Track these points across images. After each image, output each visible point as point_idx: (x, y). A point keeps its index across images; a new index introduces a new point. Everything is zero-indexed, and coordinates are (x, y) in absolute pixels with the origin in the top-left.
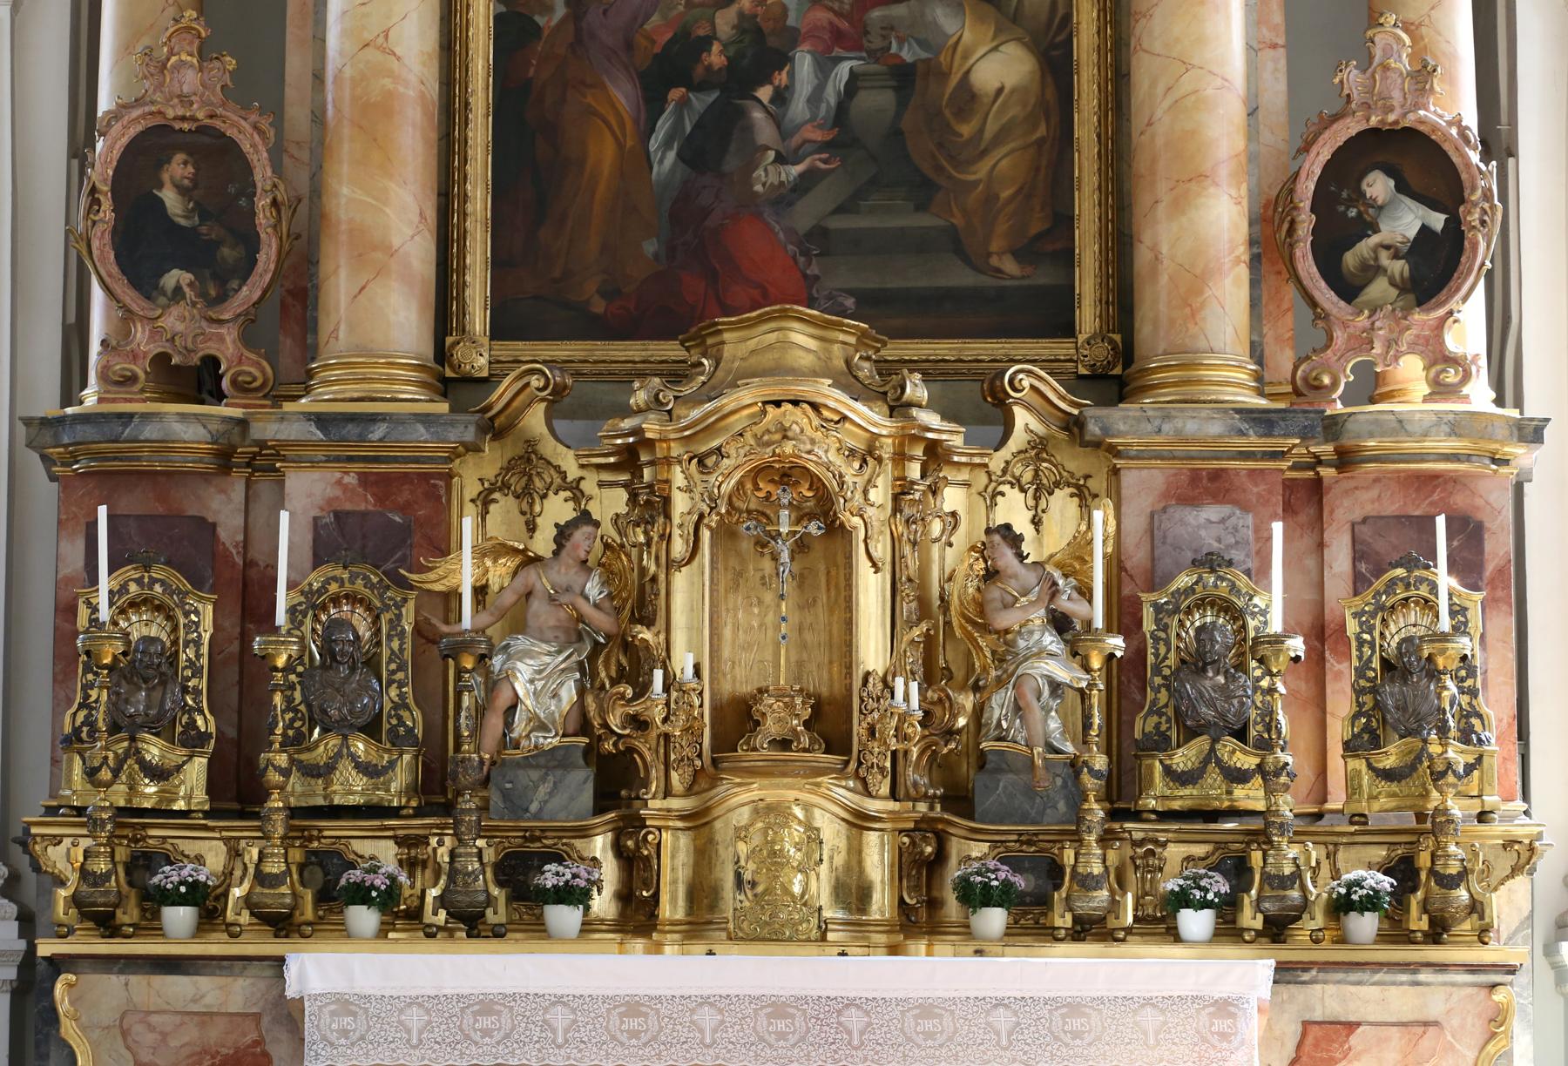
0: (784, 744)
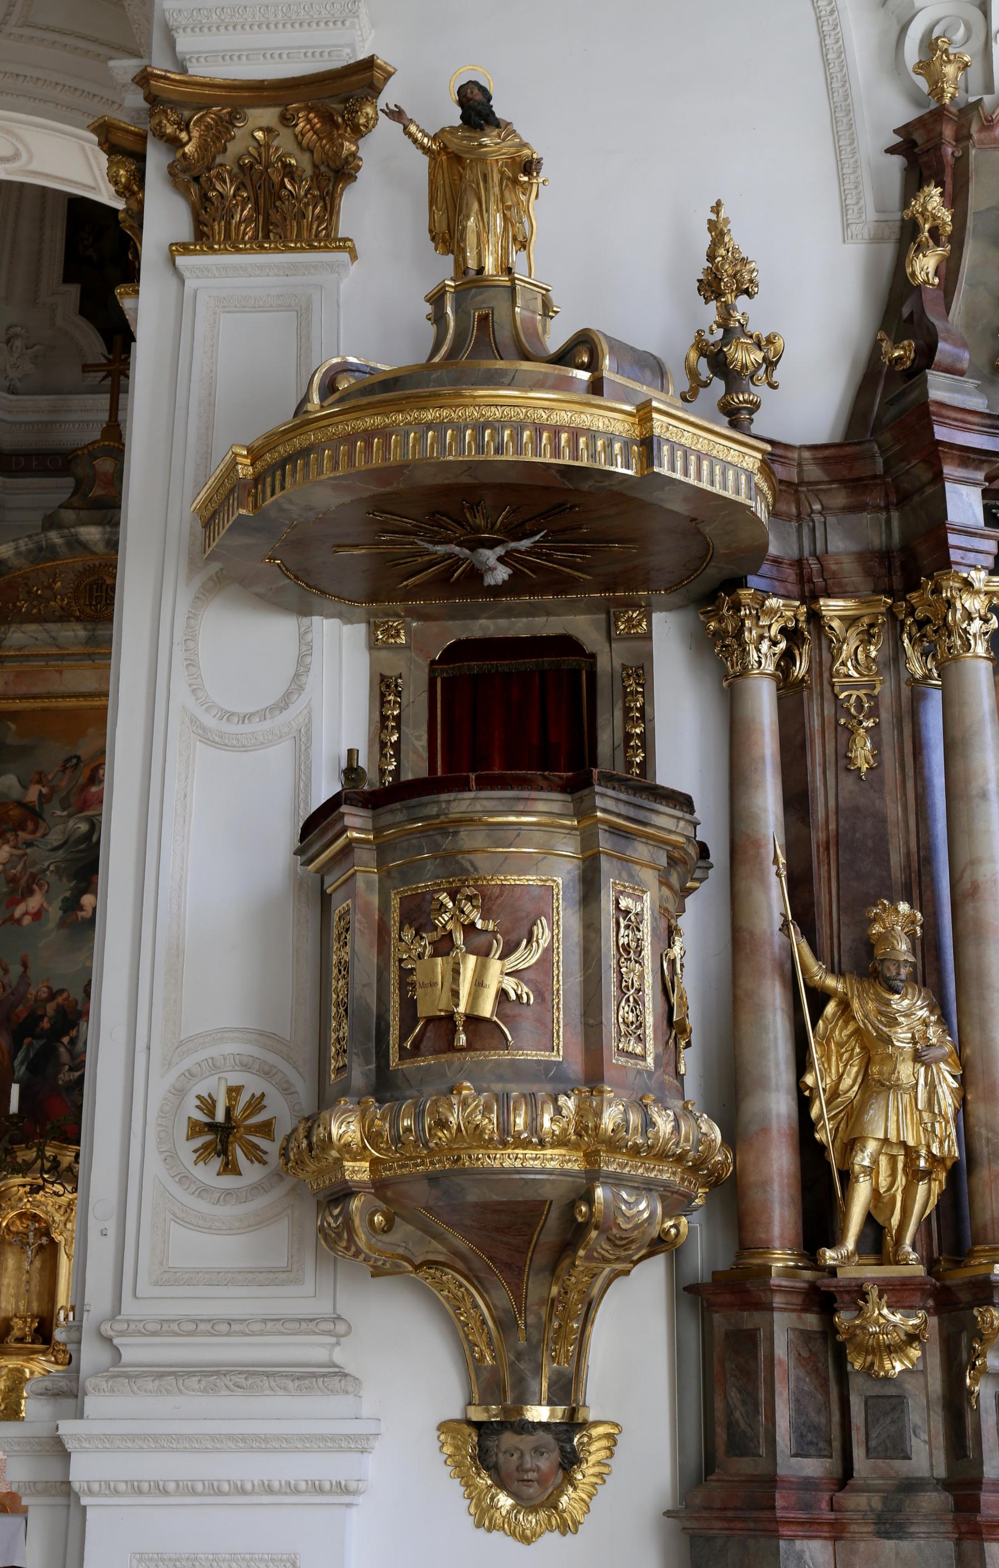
0: (20, 1340)
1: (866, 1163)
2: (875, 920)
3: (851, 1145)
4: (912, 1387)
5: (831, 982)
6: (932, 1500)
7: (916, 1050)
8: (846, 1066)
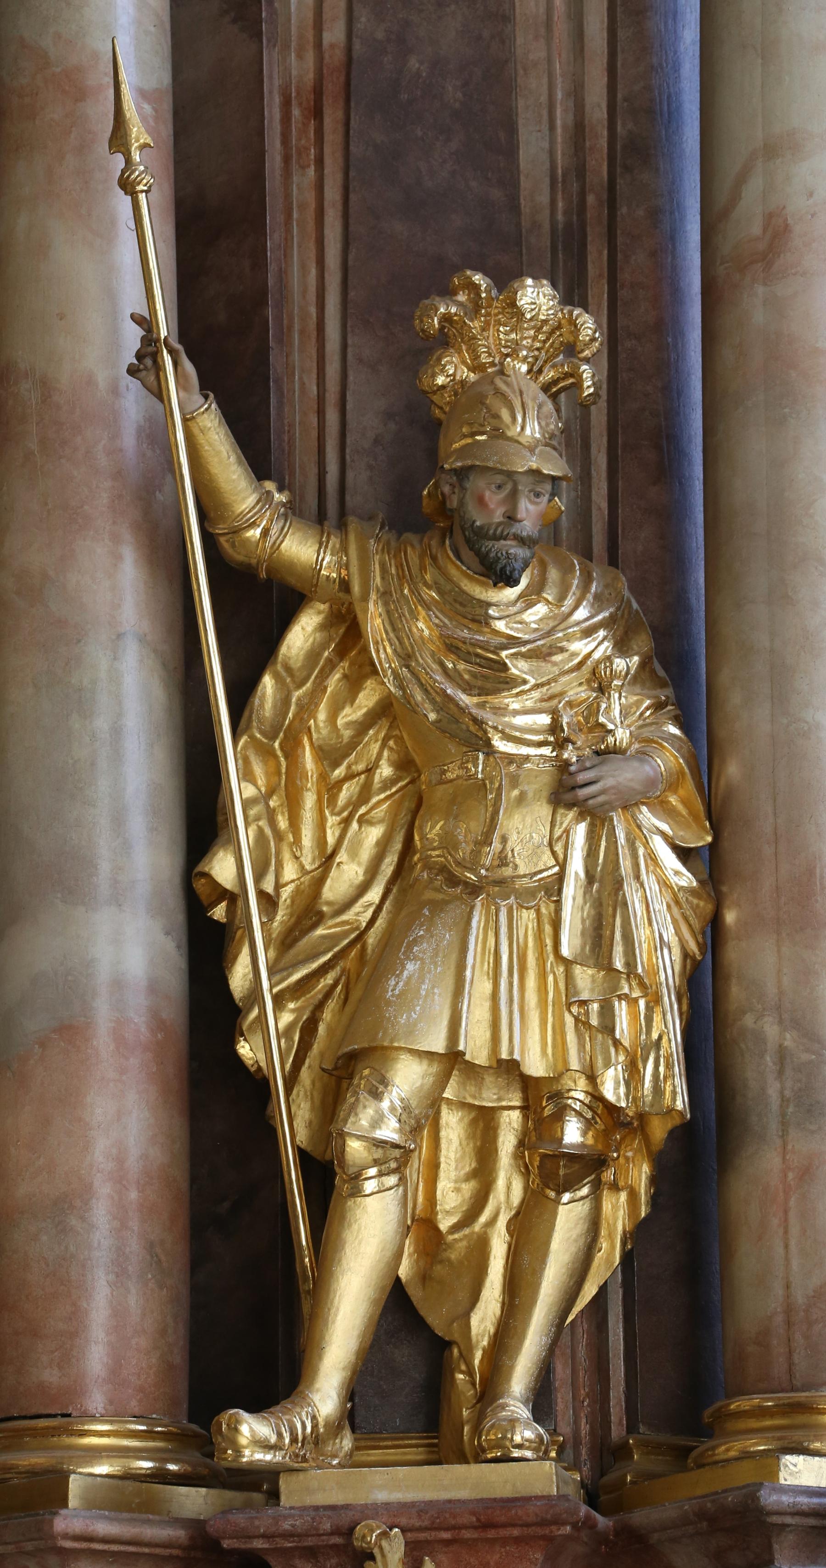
1: (389, 1131)
2: (443, 340)
3: (349, 1071)
5: (299, 548)
7: (564, 767)
8: (347, 822)
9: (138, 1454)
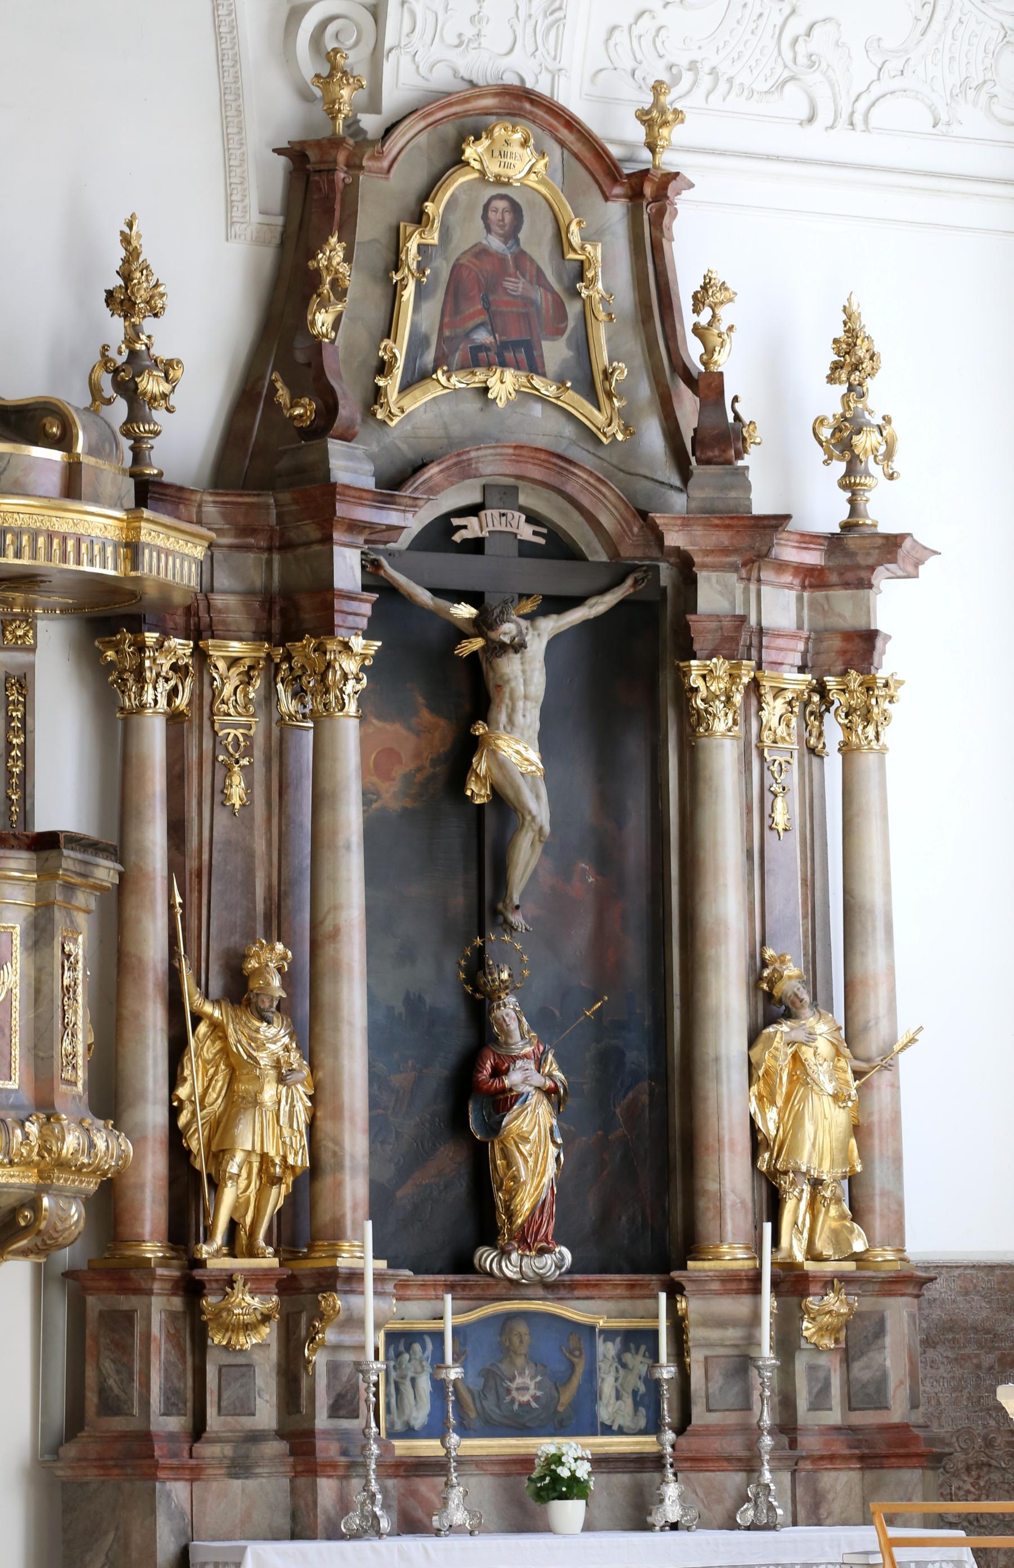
4: (257, 1357)
5: (208, 1008)
6: (276, 1447)
9: (160, 1251)
